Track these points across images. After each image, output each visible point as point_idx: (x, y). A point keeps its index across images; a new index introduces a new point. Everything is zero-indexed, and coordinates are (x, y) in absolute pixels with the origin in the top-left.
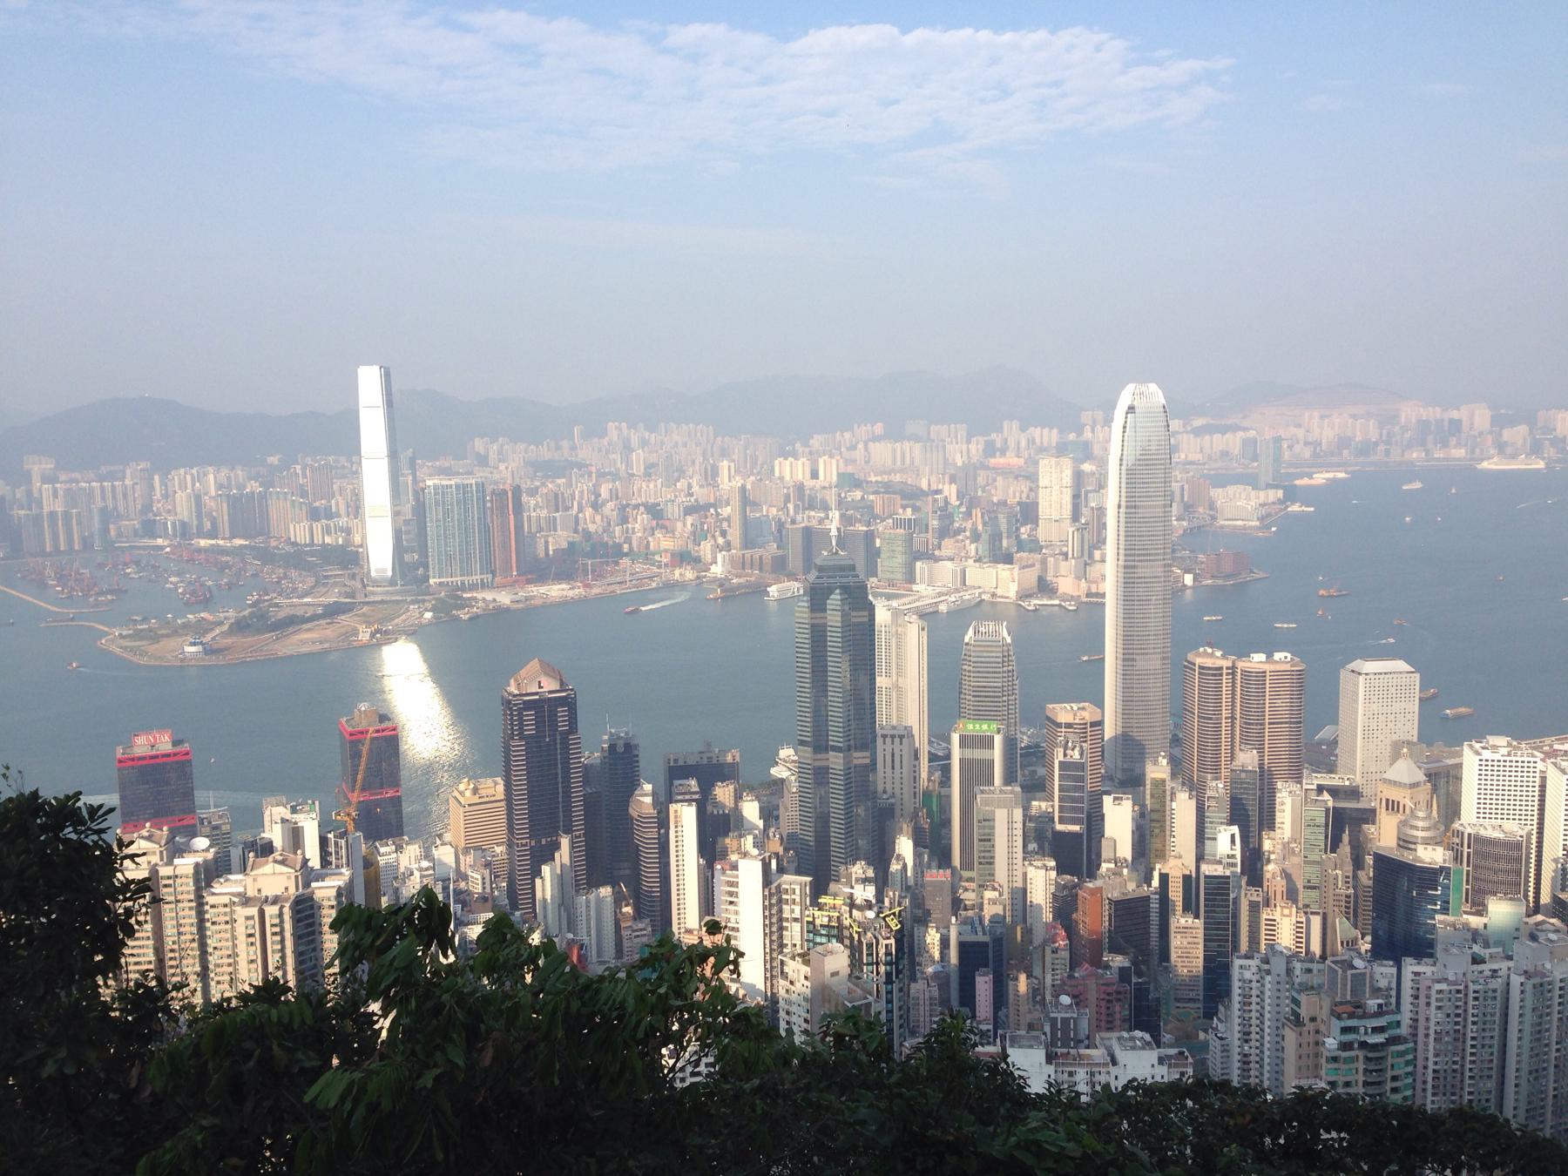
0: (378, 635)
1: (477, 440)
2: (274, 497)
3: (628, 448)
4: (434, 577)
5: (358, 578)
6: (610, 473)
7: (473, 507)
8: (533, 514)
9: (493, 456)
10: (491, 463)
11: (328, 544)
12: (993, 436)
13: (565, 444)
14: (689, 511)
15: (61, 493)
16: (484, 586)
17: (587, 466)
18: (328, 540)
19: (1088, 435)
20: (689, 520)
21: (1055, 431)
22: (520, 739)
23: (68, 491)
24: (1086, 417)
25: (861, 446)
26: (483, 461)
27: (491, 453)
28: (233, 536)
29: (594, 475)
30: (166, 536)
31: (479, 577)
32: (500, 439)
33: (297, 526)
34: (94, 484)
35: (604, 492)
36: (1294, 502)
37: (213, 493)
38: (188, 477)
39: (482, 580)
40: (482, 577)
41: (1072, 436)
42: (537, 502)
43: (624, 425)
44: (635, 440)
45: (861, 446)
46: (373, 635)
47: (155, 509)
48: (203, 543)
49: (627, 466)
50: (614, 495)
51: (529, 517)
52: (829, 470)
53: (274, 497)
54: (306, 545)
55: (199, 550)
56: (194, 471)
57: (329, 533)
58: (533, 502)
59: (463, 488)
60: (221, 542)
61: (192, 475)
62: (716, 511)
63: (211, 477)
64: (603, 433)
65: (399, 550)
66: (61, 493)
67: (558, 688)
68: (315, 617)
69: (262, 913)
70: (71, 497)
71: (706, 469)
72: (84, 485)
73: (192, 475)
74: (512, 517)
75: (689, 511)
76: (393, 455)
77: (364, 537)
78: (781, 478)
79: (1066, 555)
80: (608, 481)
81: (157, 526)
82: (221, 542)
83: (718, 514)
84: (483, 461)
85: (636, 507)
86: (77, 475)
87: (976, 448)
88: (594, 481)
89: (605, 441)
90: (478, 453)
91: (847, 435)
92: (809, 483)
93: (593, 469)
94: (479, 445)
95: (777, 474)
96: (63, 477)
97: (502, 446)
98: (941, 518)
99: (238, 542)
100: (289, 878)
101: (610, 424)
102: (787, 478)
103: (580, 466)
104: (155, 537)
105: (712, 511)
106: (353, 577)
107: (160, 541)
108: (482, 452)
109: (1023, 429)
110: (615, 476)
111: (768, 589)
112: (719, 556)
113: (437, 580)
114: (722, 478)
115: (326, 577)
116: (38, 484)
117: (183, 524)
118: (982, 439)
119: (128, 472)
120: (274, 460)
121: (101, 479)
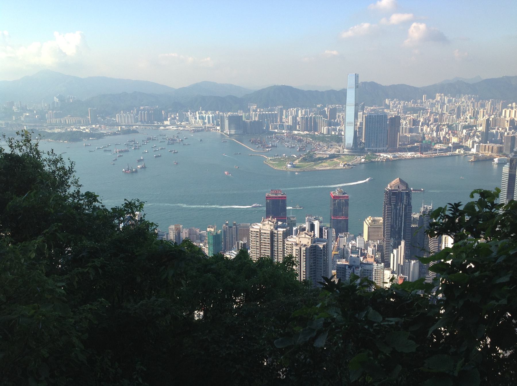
0: (346, 166)
4: (367, 147)
5: (342, 146)
6: (435, 112)
8: (404, 126)
10: (391, 107)
11: (333, 135)
14: (465, 127)
20: (465, 131)
29: (429, 113)
34: (267, 113)
37: (300, 117)
38: (293, 111)
42: (407, 123)
46: (344, 166)
47: (283, 121)
48: (296, 132)
49: (442, 110)
51: (402, 128)
54: (326, 134)
55: (295, 135)
56: (295, 109)
58: (404, 123)
61: (294, 110)
62: (476, 128)
63: (300, 111)
67: (405, 189)
68: (326, 159)
69: (300, 249)
71: (474, 111)
72: (264, 113)
73: (294, 110)
75: (465, 127)
76: (356, 105)
77: (345, 133)
80: (434, 115)
83: (477, 129)
86: (262, 110)
88: (429, 115)
93: (429, 111)
100: (309, 239)
101: (438, 94)
103: (424, 109)
105: (474, 128)
106: (340, 146)
111: (494, 159)
112: (475, 146)
114: (480, 116)
115: (331, 145)
116: (252, 112)
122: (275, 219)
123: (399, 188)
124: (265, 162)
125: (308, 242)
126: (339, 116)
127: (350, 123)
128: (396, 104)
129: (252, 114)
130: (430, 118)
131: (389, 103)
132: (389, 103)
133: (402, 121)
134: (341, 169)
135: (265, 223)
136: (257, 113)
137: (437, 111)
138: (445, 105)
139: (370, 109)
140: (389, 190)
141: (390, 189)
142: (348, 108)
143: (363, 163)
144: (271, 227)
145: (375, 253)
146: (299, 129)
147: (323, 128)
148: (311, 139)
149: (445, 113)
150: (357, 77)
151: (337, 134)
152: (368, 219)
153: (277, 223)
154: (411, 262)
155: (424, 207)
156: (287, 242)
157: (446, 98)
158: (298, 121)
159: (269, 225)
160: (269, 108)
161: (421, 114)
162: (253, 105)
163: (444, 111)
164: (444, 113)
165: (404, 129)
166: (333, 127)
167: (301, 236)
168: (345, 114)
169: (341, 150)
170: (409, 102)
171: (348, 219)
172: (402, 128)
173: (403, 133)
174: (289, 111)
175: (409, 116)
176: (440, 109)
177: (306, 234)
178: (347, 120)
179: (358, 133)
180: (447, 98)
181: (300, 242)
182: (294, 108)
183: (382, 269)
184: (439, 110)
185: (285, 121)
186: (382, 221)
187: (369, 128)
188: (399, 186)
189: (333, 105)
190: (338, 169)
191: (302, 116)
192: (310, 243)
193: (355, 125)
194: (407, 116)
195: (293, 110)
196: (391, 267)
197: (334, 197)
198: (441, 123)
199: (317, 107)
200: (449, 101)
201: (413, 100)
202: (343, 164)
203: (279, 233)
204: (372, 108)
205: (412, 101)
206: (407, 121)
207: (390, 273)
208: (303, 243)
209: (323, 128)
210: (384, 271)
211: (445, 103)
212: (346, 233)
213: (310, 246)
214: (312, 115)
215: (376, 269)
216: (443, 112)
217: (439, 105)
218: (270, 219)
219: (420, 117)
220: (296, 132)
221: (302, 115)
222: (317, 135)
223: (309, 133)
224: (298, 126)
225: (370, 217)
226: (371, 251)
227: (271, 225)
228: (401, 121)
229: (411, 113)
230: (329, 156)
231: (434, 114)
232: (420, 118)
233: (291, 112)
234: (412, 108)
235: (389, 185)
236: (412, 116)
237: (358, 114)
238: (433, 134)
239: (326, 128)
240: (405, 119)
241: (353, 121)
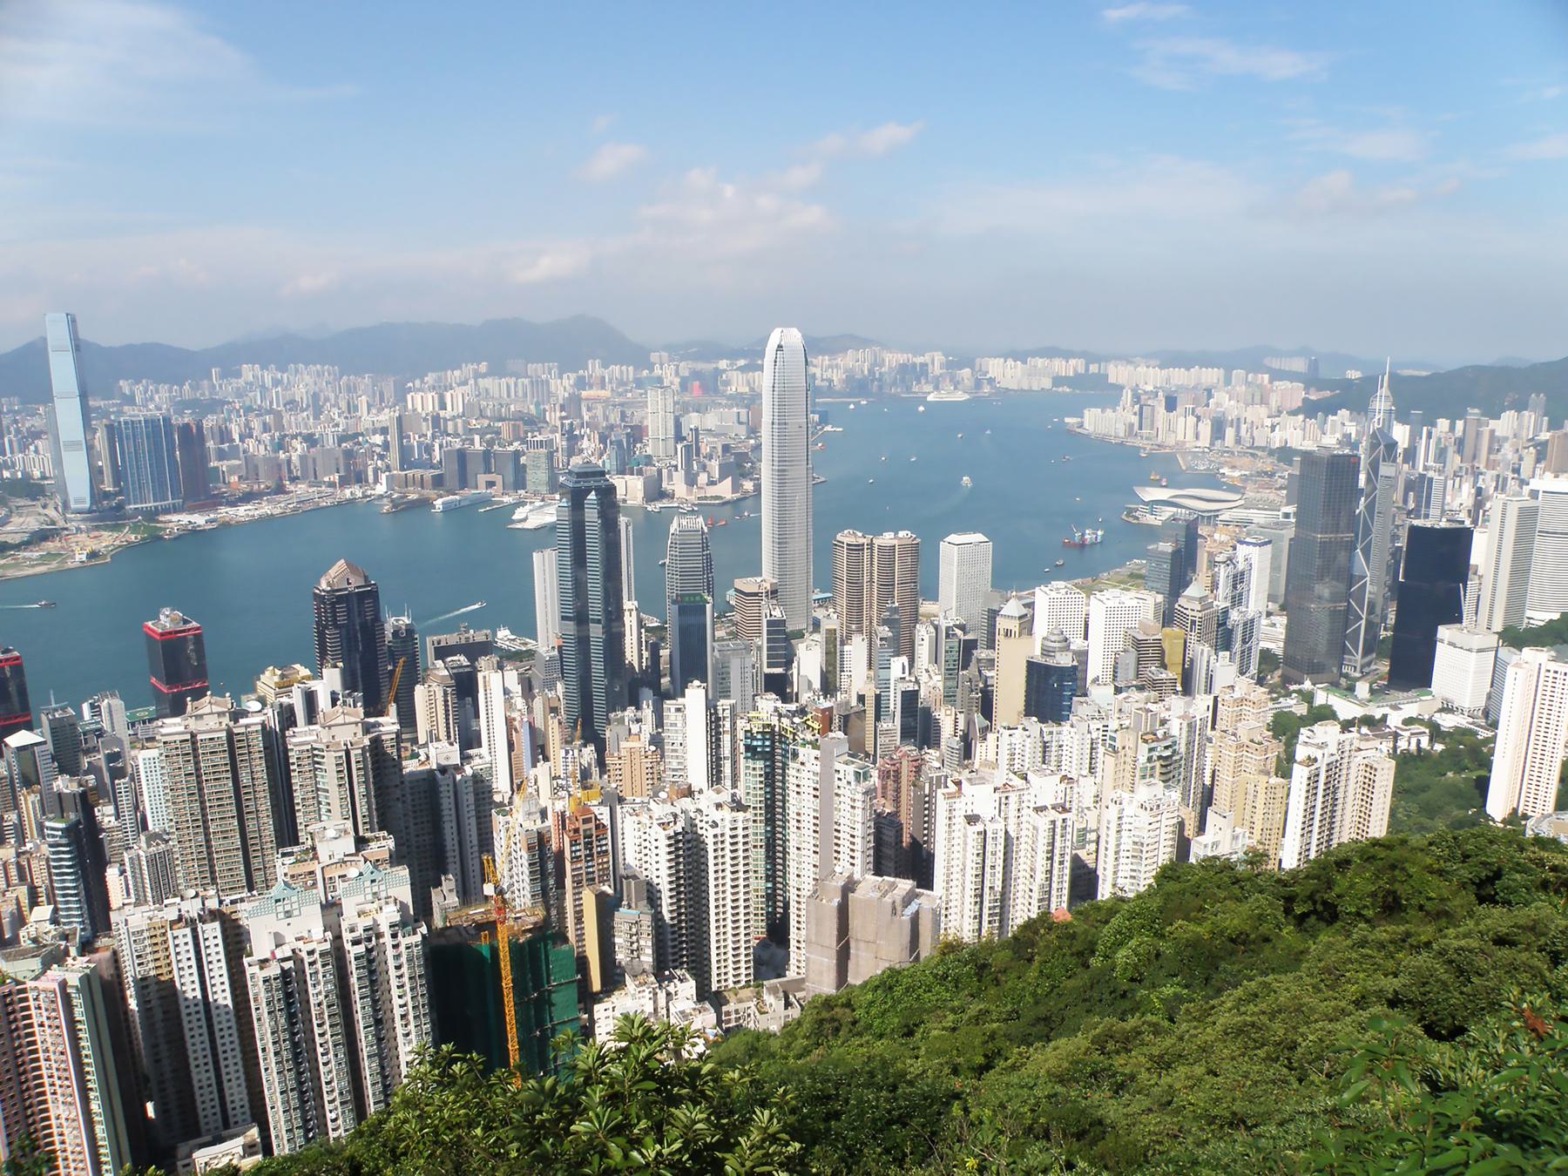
12: (581, 372)
16: (176, 510)
19: (657, 372)
21: (631, 368)
24: (654, 357)
25: (472, 382)
26: (130, 400)
35: (256, 424)
36: (827, 424)
41: (645, 372)
45: (472, 382)
52: (456, 401)
64: (238, 375)
78: (414, 410)
79: (676, 466)
84: (130, 400)
85: (295, 437)
87: (569, 380)
91: (457, 373)
92: (442, 413)
95: (410, 406)
98: (568, 439)
102: (420, 410)
109: (605, 366)
110: (261, 412)
118: (573, 376)
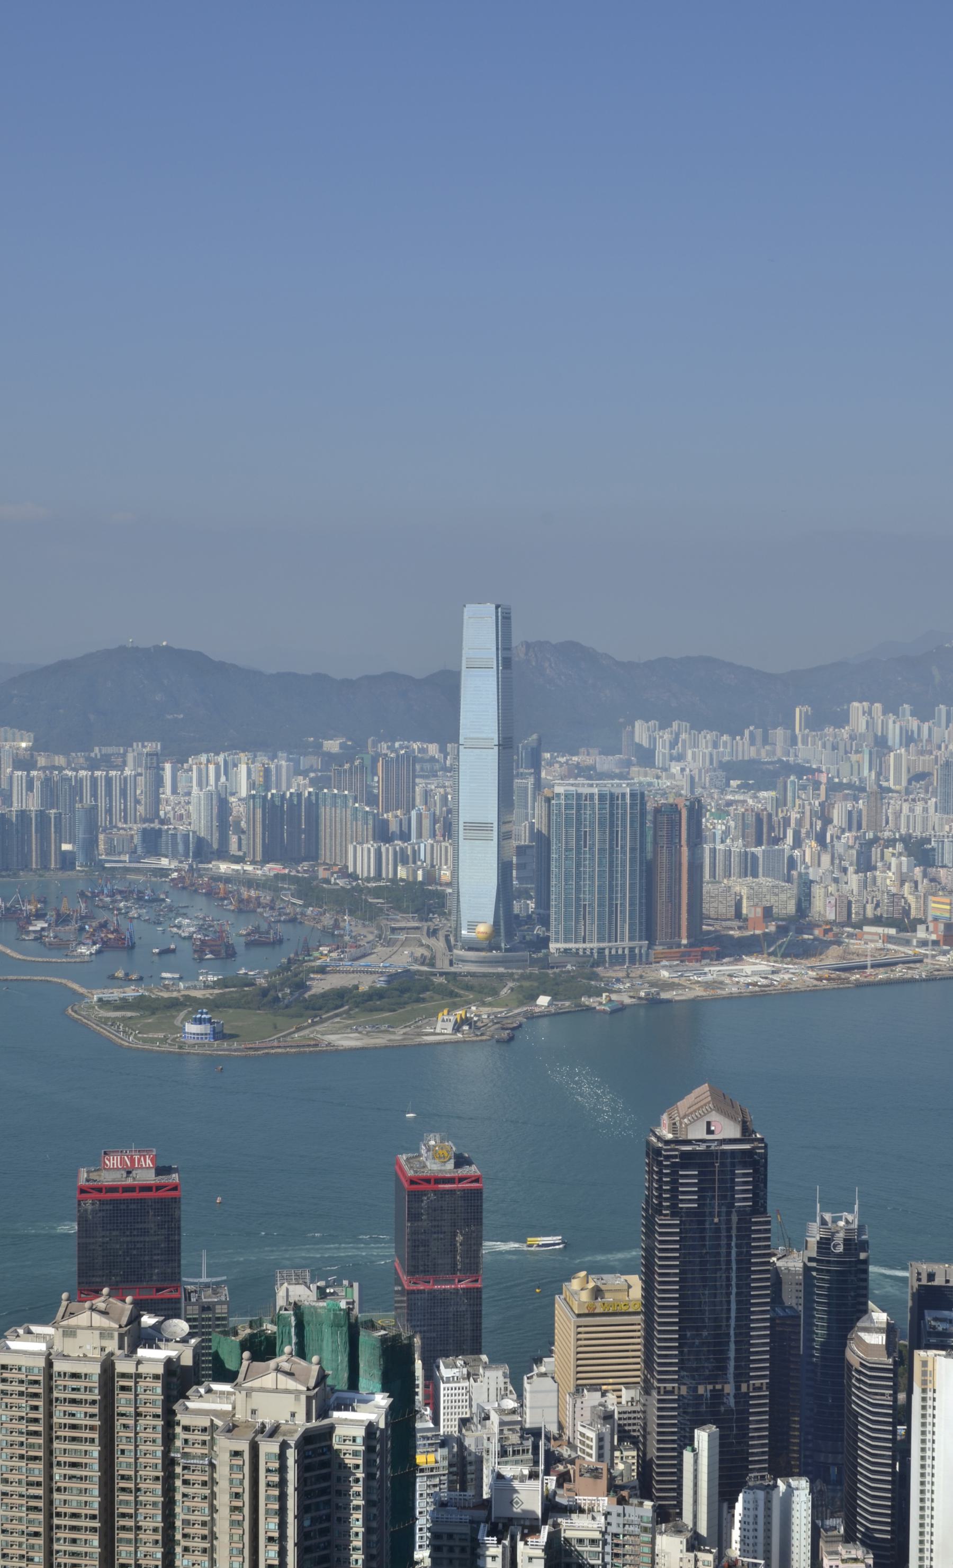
0: (466, 1028)
1: (638, 724)
2: (329, 801)
3: (881, 744)
4: (557, 941)
5: (441, 934)
6: (850, 786)
7: (624, 831)
8: (719, 847)
9: (662, 750)
10: (659, 760)
11: (402, 880)
13: (779, 734)
15: (37, 784)
17: (811, 771)
18: (402, 873)
22: (674, 1215)
23: (47, 782)
26: (646, 757)
27: (659, 743)
28: (267, 859)
29: (823, 787)
30: (174, 856)
31: (627, 943)
32: (675, 725)
33: (359, 848)
34: (82, 773)
37: (244, 793)
38: (212, 767)
39: (632, 949)
40: (633, 944)
42: (728, 828)
43: (878, 706)
44: (893, 732)
46: (457, 1028)
47: (162, 813)
48: (224, 867)
49: (879, 774)
50: (853, 822)
51: (713, 851)
53: (329, 801)
54: (368, 879)
55: (218, 878)
56: (221, 759)
57: (405, 862)
58: (720, 828)
59: (610, 799)
60: (249, 868)
63: (243, 768)
64: (842, 720)
65: (505, 893)
66: (37, 784)
70: (50, 791)
72: (69, 773)
73: (217, 765)
74: (685, 850)
76: (506, 745)
77: (455, 872)
80: (846, 798)
81: (164, 839)
82: (249, 868)
84: (646, 757)
85: (891, 843)
86: (60, 760)
88: (823, 798)
89: (845, 733)
90: (639, 746)
93: (823, 778)
94: (641, 732)
96: (42, 761)
97: (677, 735)
99: (272, 869)
101: (856, 704)
103: (801, 770)
104: (158, 854)
106: (433, 933)
107: (165, 862)
108: (645, 743)
110: (857, 790)
113: (562, 946)
115: (393, 930)
116: (9, 770)
117: (200, 841)
119: (130, 757)
120: (332, 746)
121: (93, 765)
122: (129, 1299)
123: (709, 1132)
124: (73, 1011)
125: (293, 1415)
126: (427, 794)
127: (478, 827)
128: (680, 745)
129: (11, 777)
130: (829, 812)
131: (653, 740)
132: (653, 740)
133: (707, 821)
134: (445, 1043)
135: (73, 1321)
136: (34, 773)
137: (855, 779)
138: (892, 754)
139: (567, 763)
140: (667, 1142)
141: (670, 1136)
142: (467, 757)
143: (542, 1015)
144: (105, 1343)
145: (613, 1449)
146: (241, 854)
147: (355, 848)
148: (300, 902)
149: (892, 787)
150: (503, 618)
151: (420, 878)
152: (575, 1284)
153: (135, 1319)
154: (775, 1486)
155: (824, 1222)
156: (183, 1419)
157: (891, 722)
158: (234, 813)
159: (97, 1333)
160: (93, 751)
161: (789, 794)
162: (14, 734)
163: (888, 780)
164: (889, 790)
165: (720, 858)
166: (399, 842)
167: (256, 1383)
168: (456, 791)
169: (438, 956)
170: (738, 738)
171: (479, 1290)
172: (713, 851)
173: (715, 878)
174: (191, 770)
175: (737, 797)
176: (870, 770)
177: (278, 1370)
178: (465, 815)
179: (514, 872)
180: (894, 722)
181: (254, 1412)
182: (217, 754)
183: (645, 1530)
184: (866, 773)
185: (171, 815)
186: (637, 1292)
187: (566, 850)
188: (709, 1124)
189: (397, 745)
190: (426, 1045)
191: (253, 792)
192: (301, 1418)
193: (504, 837)
194: (730, 797)
195: (208, 761)
196: (687, 1518)
197: (412, 1181)
198: (879, 834)
199: (325, 749)
200: (908, 739)
201: (752, 728)
202: (452, 1018)
203: (142, 1369)
204: (575, 759)
205: (747, 732)
206: (732, 824)
207: (684, 1547)
208: (267, 1421)
209: (355, 848)
210: (653, 1542)
211: (890, 743)
212: (470, 1358)
213: (300, 1431)
214: (299, 785)
215: (619, 1530)
216: (885, 784)
217: (866, 751)
218: (100, 1303)
219: (785, 805)
220: (224, 867)
221: (252, 786)
222: (327, 881)
223: (286, 871)
224: (234, 839)
225: (583, 1274)
226: (594, 1444)
227: (104, 1333)
228: (704, 820)
229: (744, 787)
230: (388, 982)
231: (846, 792)
232: (785, 809)
233: (200, 771)
234: (752, 762)
235: (665, 1118)
236: (750, 802)
237: (512, 782)
238: (846, 883)
239: (369, 850)
240: (722, 813)
241: (491, 815)
